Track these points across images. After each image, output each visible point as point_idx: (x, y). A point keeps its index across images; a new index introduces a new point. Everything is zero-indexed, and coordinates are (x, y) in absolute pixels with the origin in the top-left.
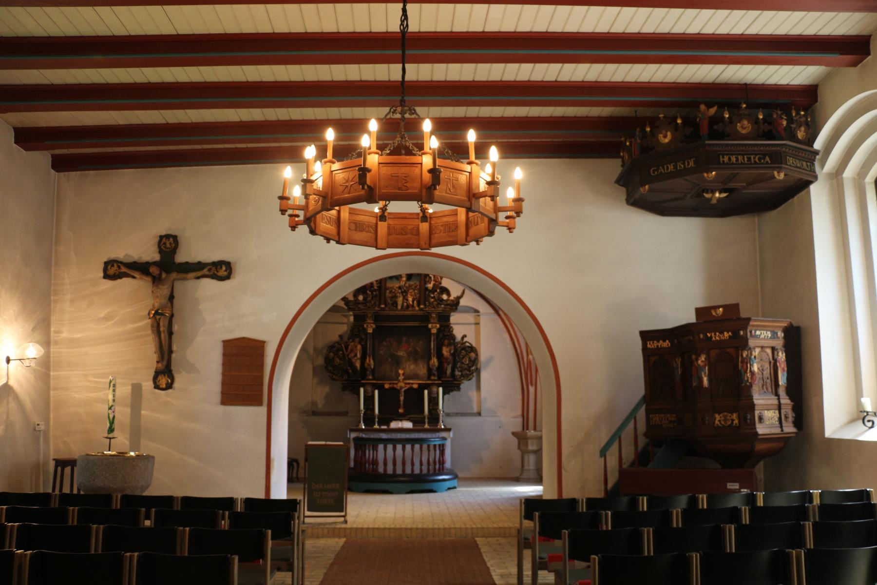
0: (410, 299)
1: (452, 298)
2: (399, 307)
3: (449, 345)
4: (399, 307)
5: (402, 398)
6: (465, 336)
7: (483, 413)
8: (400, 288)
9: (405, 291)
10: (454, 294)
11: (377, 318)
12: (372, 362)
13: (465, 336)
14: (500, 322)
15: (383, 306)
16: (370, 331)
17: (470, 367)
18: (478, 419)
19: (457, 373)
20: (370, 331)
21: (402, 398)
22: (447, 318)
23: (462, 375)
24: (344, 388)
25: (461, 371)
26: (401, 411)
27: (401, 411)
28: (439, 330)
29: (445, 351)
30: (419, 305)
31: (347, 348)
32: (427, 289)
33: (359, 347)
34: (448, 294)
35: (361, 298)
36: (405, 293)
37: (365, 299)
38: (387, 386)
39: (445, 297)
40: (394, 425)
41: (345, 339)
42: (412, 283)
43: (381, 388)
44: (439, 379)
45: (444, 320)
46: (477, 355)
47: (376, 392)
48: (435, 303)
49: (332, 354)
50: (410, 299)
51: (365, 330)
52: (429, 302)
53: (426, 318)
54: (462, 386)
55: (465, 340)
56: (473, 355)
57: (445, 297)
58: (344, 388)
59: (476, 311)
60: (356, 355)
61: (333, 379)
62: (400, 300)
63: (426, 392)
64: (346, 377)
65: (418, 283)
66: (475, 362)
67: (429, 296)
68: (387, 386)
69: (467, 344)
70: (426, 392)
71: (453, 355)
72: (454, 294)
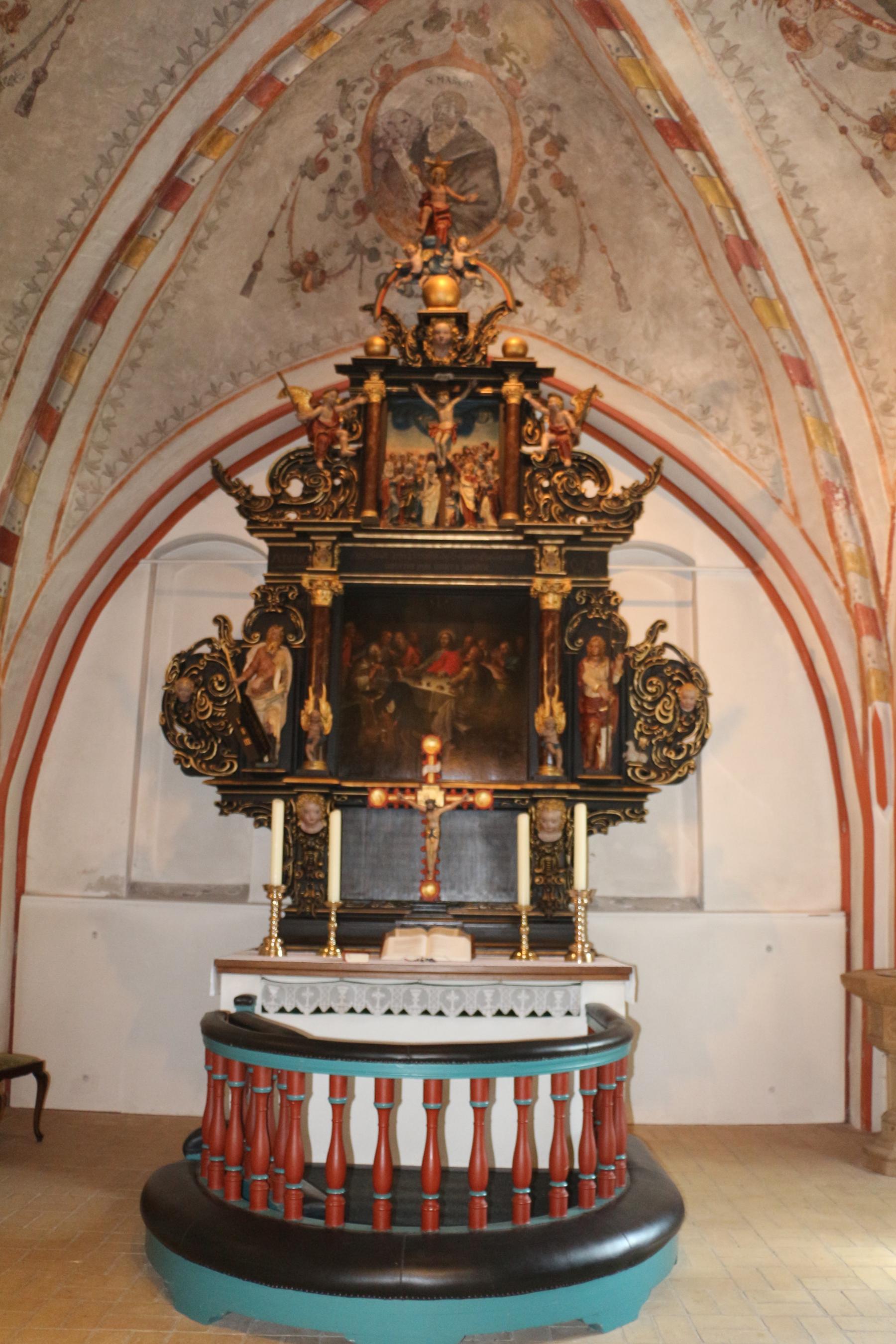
0: (468, 493)
1: (615, 490)
2: (429, 518)
3: (610, 654)
4: (429, 518)
6: (660, 626)
7: (709, 902)
8: (432, 457)
9: (450, 468)
10: (623, 477)
11: (348, 562)
12: (325, 707)
13: (660, 626)
14: (763, 597)
15: (370, 513)
16: (323, 598)
17: (679, 737)
18: (693, 919)
20: (323, 598)
22: (598, 565)
23: (649, 766)
25: (648, 750)
28: (569, 601)
29: (595, 678)
30: (497, 512)
31: (239, 661)
32: (526, 460)
33: (285, 658)
34: (602, 477)
35: (295, 488)
36: (448, 471)
37: (309, 492)
39: (590, 489)
41: (237, 633)
42: (471, 442)
45: (588, 562)
46: (705, 692)
48: (556, 508)
49: (185, 684)
50: (468, 493)
51: (305, 596)
52: (534, 503)
53: (525, 563)
54: (651, 803)
55: (662, 637)
56: (689, 693)
57: (590, 489)
59: (686, 560)
60: (269, 684)
62: (431, 499)
65: (494, 444)
66: (695, 718)
67: (533, 482)
69: (669, 655)
71: (621, 690)
72: (623, 477)
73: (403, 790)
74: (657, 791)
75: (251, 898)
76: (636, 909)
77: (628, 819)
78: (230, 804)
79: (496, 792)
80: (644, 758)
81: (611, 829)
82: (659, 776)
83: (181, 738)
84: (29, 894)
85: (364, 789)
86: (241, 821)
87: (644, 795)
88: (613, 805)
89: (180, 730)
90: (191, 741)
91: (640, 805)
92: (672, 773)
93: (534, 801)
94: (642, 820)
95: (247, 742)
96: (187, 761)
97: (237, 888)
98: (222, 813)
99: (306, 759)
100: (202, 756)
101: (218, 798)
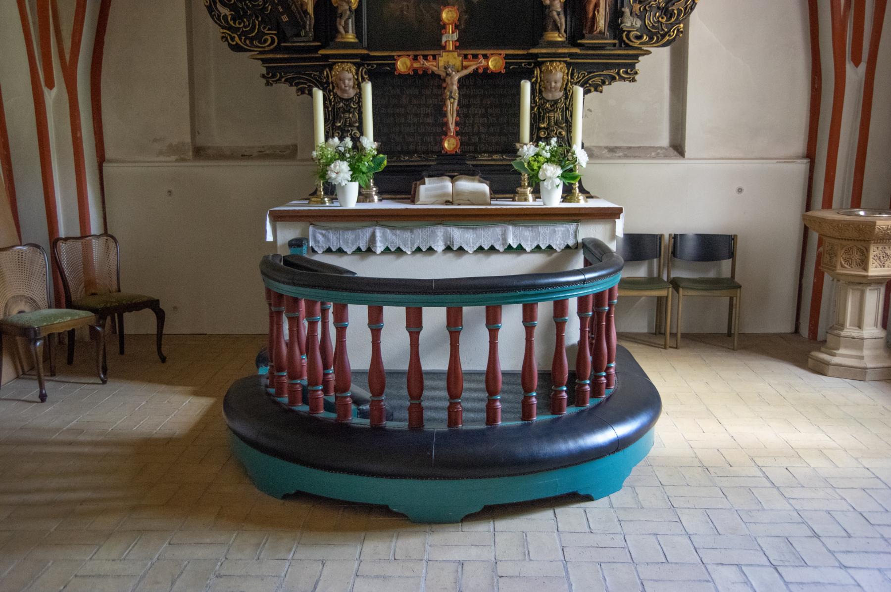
5: (452, 107)
19: (630, 23)
21: (452, 107)
24: (272, 76)
26: (449, 145)
27: (449, 145)
38: (403, 65)
40: (432, 191)
43: (382, 76)
44: (572, 41)
47: (368, 88)
58: (272, 76)
61: (237, 48)
63: (526, 86)
64: (270, 35)
68: (403, 65)
70: (526, 86)
73: (425, 57)
74: (648, 53)
75: (299, 155)
76: (626, 156)
77: (622, 79)
78: (274, 76)
79: (507, 57)
80: (639, 23)
81: (605, 88)
82: (651, 39)
83: (225, 17)
84: (110, 161)
85: (391, 58)
86: (286, 91)
87: (636, 57)
88: (607, 66)
89: (224, 11)
90: (234, 19)
91: (632, 66)
92: (663, 36)
93: (539, 65)
94: (634, 80)
95: (285, 18)
96: (233, 39)
97: (287, 147)
98: (268, 84)
99: (338, 32)
100: (244, 33)
101: (264, 71)
